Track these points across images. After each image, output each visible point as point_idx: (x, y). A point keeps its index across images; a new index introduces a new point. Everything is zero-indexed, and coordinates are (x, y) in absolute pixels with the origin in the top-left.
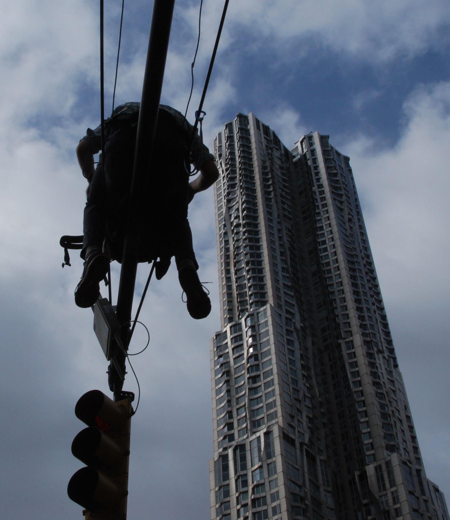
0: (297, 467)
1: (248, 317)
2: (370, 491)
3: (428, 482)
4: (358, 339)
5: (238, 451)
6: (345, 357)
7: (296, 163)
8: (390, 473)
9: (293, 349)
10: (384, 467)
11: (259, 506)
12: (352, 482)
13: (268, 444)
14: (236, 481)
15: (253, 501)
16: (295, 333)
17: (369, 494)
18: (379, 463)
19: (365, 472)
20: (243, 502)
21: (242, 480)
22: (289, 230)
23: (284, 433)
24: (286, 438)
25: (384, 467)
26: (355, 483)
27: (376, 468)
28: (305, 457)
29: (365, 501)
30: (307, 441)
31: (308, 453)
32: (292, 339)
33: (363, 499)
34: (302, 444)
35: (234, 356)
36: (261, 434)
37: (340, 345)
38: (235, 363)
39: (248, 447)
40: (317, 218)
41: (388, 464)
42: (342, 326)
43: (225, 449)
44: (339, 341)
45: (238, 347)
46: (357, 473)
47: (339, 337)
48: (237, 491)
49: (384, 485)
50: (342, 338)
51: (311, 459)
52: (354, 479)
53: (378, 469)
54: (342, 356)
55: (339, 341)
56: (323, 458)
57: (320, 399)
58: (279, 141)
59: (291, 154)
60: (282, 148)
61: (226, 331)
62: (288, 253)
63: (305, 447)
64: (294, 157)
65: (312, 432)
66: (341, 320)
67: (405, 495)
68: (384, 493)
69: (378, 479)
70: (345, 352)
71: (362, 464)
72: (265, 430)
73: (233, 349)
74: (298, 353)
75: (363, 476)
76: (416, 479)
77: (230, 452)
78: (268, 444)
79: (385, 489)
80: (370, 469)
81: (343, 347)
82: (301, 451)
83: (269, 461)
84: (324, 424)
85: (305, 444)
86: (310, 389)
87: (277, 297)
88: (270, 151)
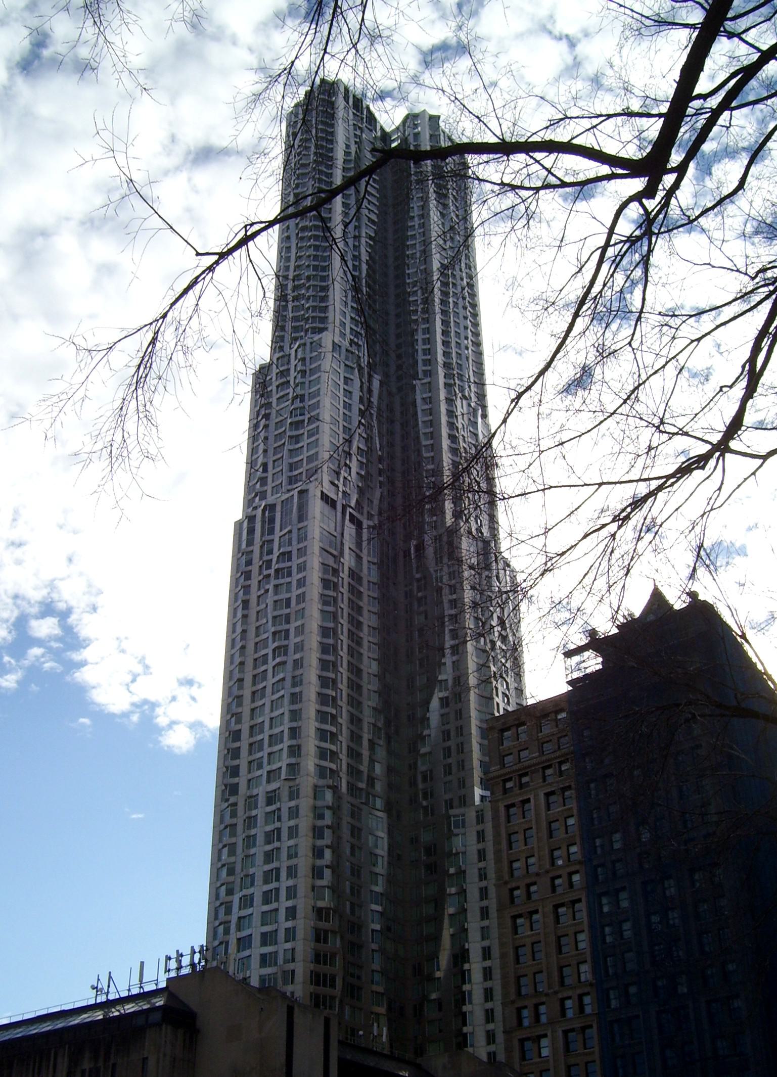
0: (335, 534)
1: (299, 347)
6: (419, 401)
9: (351, 390)
11: (283, 577)
12: (407, 553)
14: (261, 547)
15: (277, 571)
16: (356, 370)
20: (265, 573)
21: (267, 546)
22: (370, 238)
28: (347, 522)
29: (418, 576)
30: (353, 504)
32: (352, 377)
34: (344, 507)
35: (278, 396)
40: (410, 224)
43: (255, 508)
47: (416, 377)
48: (261, 558)
53: (438, 539)
56: (371, 523)
57: (380, 453)
58: (375, 119)
60: (378, 128)
62: (364, 267)
63: (349, 510)
65: (361, 491)
71: (422, 532)
73: (278, 387)
74: (357, 394)
75: (420, 548)
77: (259, 512)
83: (301, 525)
84: (380, 482)
85: (350, 507)
88: (358, 133)
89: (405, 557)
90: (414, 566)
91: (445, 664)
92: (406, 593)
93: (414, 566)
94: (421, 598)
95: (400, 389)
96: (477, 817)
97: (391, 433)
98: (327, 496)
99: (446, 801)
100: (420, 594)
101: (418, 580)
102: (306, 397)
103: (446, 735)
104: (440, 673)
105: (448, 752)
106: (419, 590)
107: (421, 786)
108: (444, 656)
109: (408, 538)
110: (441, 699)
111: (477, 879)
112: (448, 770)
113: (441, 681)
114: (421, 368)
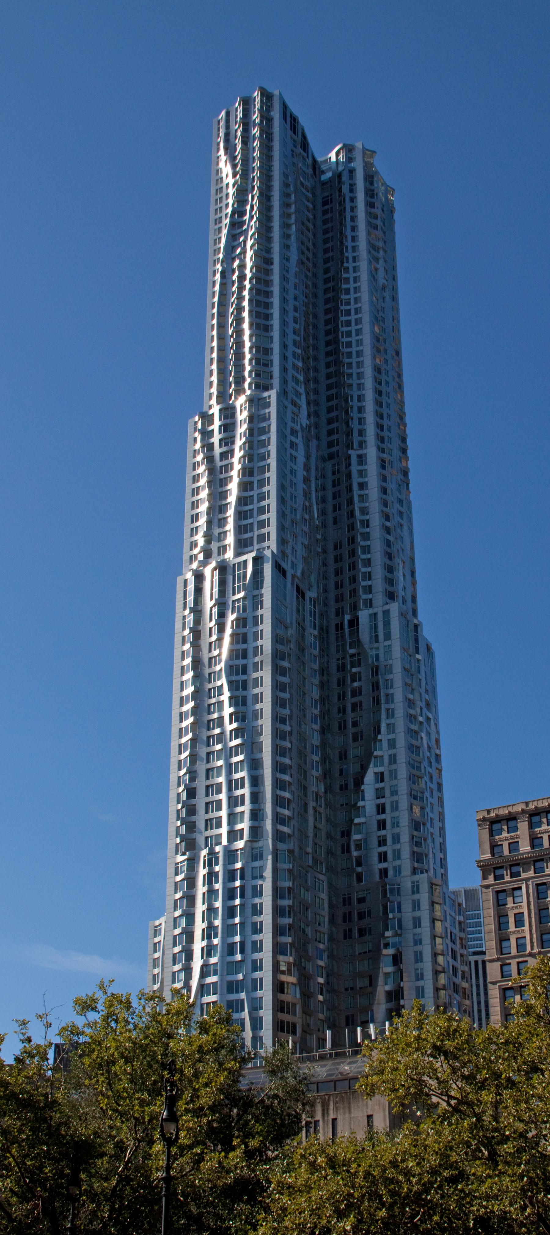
2: (358, 640)
3: (423, 636)
4: (371, 452)
5: (216, 573)
7: (324, 184)
8: (387, 624)
10: (380, 617)
12: (339, 627)
13: (258, 573)
17: (358, 643)
18: (375, 610)
19: (358, 619)
23: (276, 562)
24: (278, 569)
25: (380, 617)
26: (343, 628)
27: (370, 615)
28: (295, 593)
29: (352, 651)
30: (299, 574)
31: (298, 587)
33: (350, 648)
34: (294, 576)
36: (249, 557)
37: (349, 457)
38: (221, 460)
39: (230, 571)
41: (386, 613)
42: (355, 433)
44: (350, 452)
45: (228, 441)
46: (347, 617)
47: (350, 446)
49: (377, 637)
50: (353, 448)
51: (301, 594)
52: (342, 624)
54: (350, 472)
55: (350, 452)
59: (320, 168)
61: (213, 414)
63: (296, 580)
64: (323, 172)
66: (355, 426)
67: (399, 652)
68: (376, 645)
69: (371, 629)
70: (355, 468)
71: (355, 608)
72: (254, 554)
75: (354, 623)
76: (412, 634)
78: (258, 573)
79: (377, 641)
80: (364, 615)
81: (354, 460)
82: (293, 584)
86: (307, 509)
87: (284, 381)
89: (337, 630)
90: (348, 641)
91: (381, 740)
92: (338, 666)
93: (348, 641)
94: (355, 674)
95: (331, 457)
96: (413, 887)
97: (324, 500)
98: (280, 566)
99: (380, 870)
100: (354, 670)
101: (352, 656)
102: (255, 458)
103: (381, 809)
104: (375, 749)
105: (382, 825)
106: (353, 666)
107: (355, 854)
108: (379, 733)
109: (340, 613)
110: (376, 773)
111: (412, 944)
112: (382, 842)
113: (376, 757)
114: (356, 439)
